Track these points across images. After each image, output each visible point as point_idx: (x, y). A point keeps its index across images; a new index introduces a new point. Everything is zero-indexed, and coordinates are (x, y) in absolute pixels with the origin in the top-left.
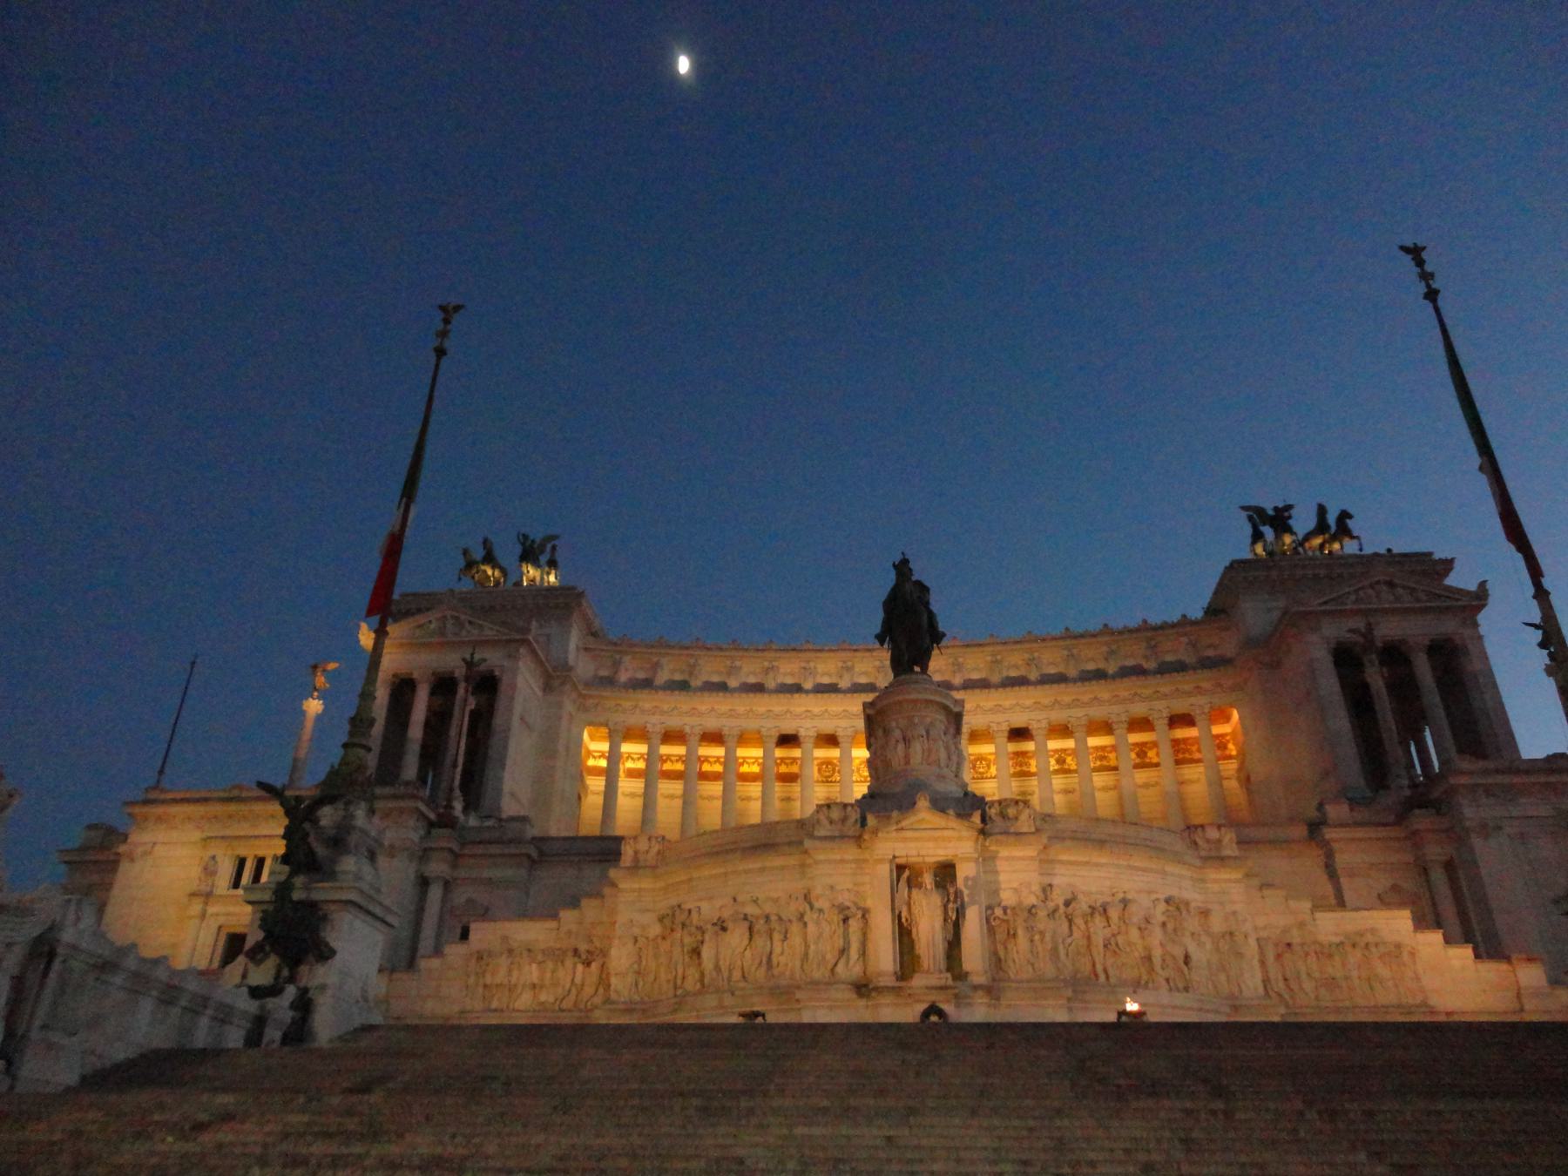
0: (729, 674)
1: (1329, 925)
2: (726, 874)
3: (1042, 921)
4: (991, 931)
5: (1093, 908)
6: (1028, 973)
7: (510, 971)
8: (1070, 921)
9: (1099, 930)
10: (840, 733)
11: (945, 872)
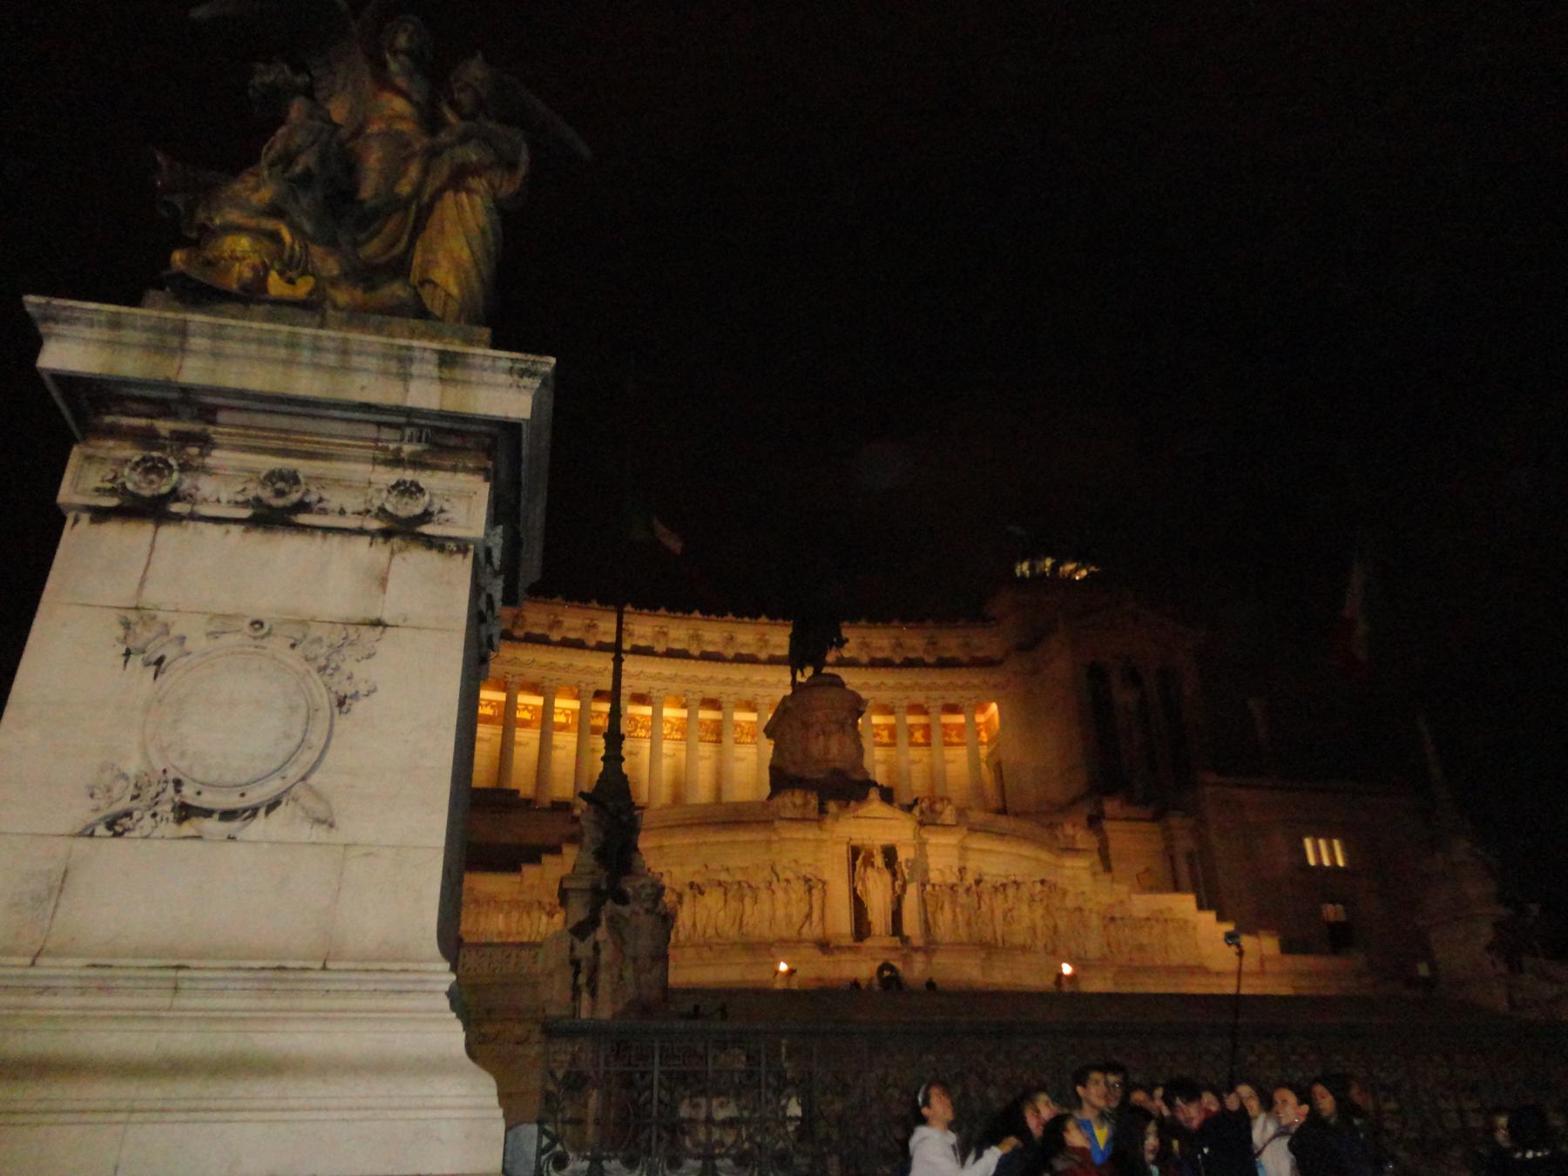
0: (551, 627)
1: (1143, 904)
2: (698, 845)
3: (963, 899)
4: (924, 902)
5: (996, 889)
6: (947, 939)
7: (477, 922)
10: (655, 693)
11: (890, 853)
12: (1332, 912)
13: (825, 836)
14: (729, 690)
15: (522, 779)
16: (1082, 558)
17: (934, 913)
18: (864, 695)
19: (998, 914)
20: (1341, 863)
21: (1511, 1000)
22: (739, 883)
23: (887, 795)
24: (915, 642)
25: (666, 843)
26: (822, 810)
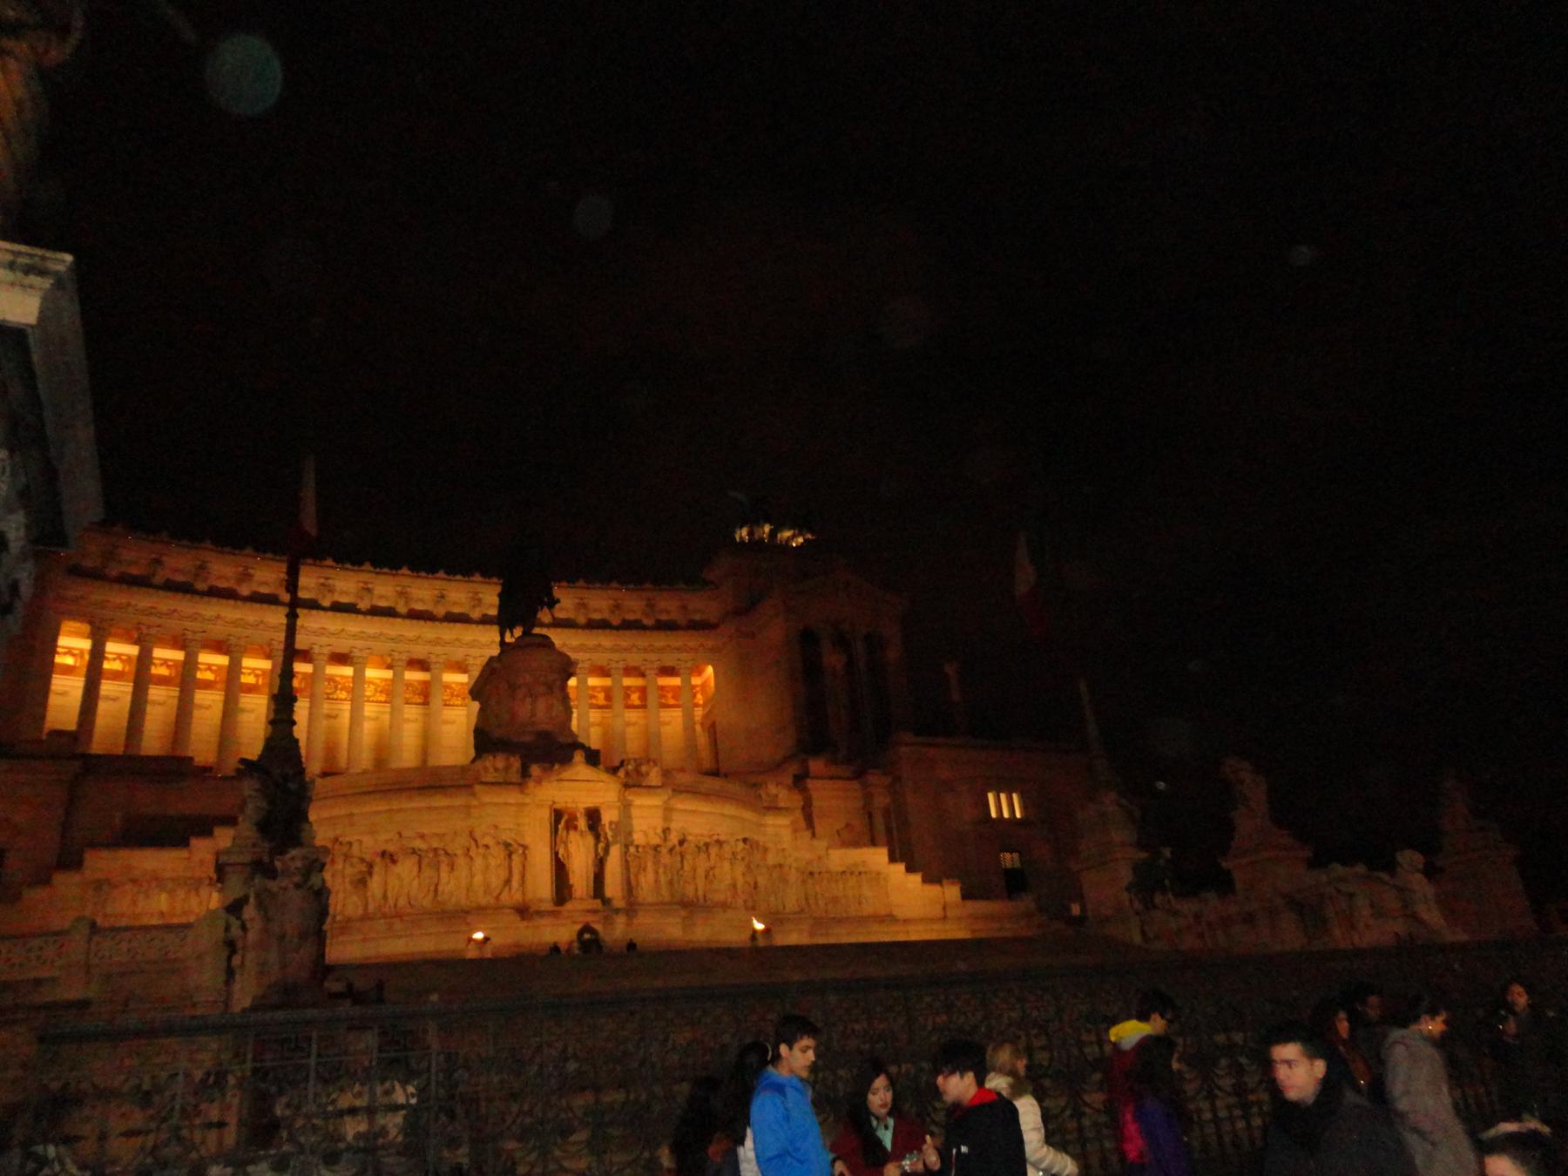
1: (840, 858)
2: (390, 811)
3: (665, 858)
4: (626, 865)
6: (650, 899)
7: (134, 903)
8: (682, 857)
9: (702, 864)
10: (357, 653)
11: (593, 816)
12: (1009, 860)
13: (527, 800)
14: (438, 650)
15: (202, 744)
16: (799, 526)
17: (636, 876)
18: (573, 656)
19: (701, 872)
20: (1018, 815)
21: (1143, 933)
22: (435, 850)
23: (593, 758)
24: (633, 604)
25: (356, 810)
26: (525, 773)
